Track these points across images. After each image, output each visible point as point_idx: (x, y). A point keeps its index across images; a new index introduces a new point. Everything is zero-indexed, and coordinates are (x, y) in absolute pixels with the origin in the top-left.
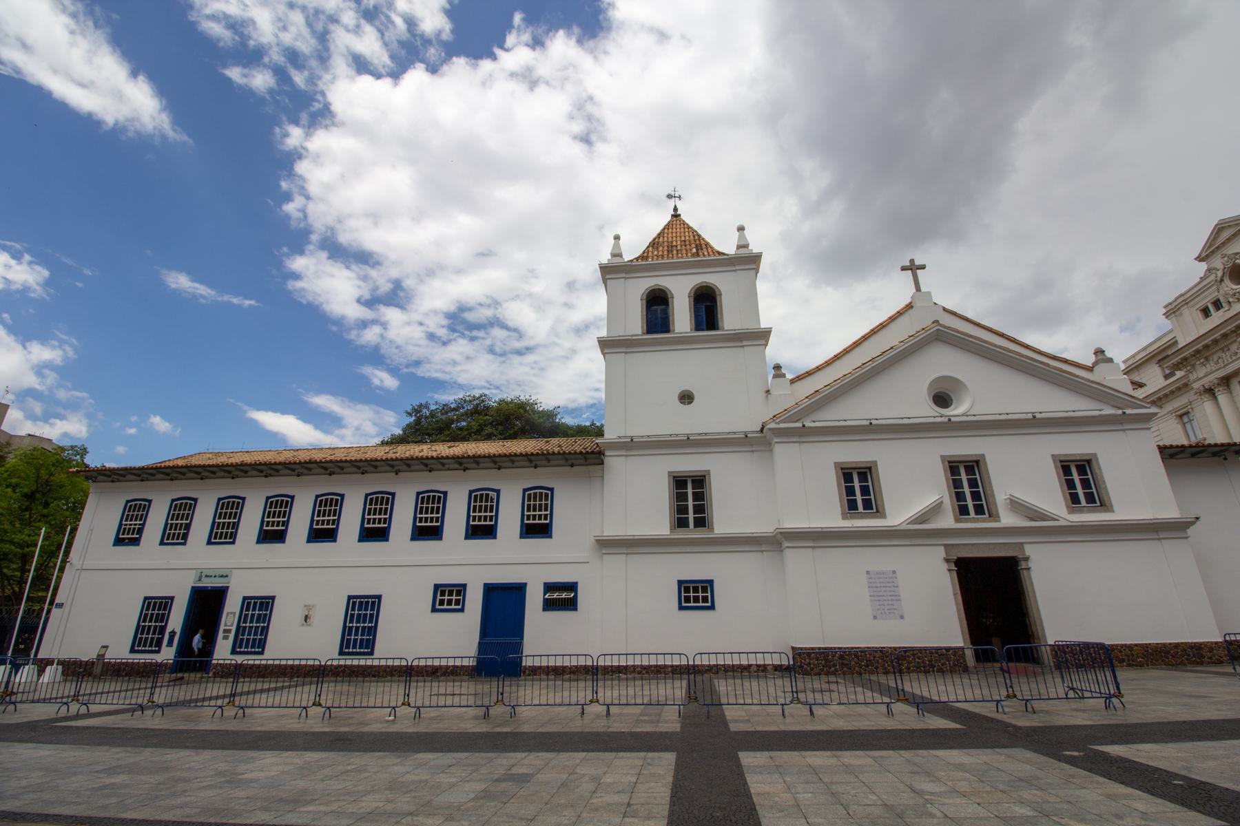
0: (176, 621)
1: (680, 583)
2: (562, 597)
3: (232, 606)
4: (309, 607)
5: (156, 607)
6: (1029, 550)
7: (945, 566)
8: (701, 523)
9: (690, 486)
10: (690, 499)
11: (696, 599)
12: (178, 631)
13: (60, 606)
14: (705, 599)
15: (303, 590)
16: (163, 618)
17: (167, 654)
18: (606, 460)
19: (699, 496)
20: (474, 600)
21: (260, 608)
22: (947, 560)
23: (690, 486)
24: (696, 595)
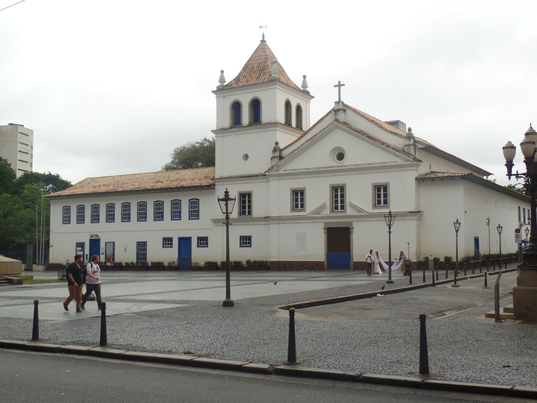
1: (241, 237)
3: (102, 245)
6: (355, 225)
7: (323, 231)
8: (250, 213)
13: (52, 246)
18: (217, 187)
22: (324, 229)
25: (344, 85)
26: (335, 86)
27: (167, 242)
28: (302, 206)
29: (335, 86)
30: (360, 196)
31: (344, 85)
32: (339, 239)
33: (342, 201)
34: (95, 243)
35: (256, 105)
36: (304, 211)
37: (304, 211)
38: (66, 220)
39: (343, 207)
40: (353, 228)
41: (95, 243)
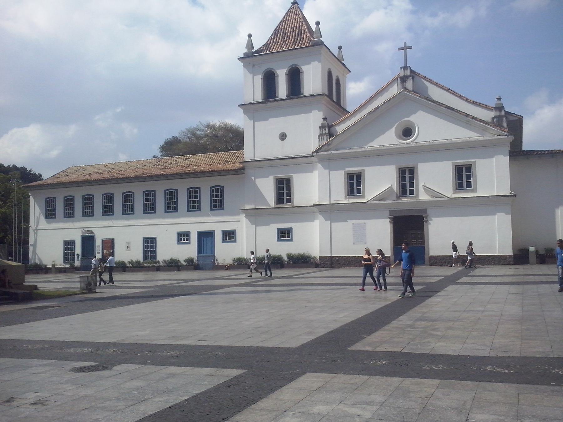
0: (78, 250)
2: (229, 236)
3: (98, 243)
4: (128, 243)
5: (69, 245)
8: (289, 201)
9: (285, 183)
10: (284, 189)
11: (285, 237)
12: (80, 254)
14: (289, 237)
15: (126, 235)
16: (73, 248)
17: (78, 263)
19: (289, 188)
20: (194, 238)
21: (109, 245)
23: (285, 183)
24: (285, 234)
25: (411, 47)
26: (400, 49)
27: (183, 237)
28: (359, 191)
29: (400, 49)
30: (435, 179)
31: (411, 47)
32: (409, 228)
33: (412, 185)
34: (88, 241)
35: (295, 77)
36: (363, 197)
37: (363, 197)
38: (50, 214)
39: (412, 192)
40: (427, 217)
41: (88, 241)
